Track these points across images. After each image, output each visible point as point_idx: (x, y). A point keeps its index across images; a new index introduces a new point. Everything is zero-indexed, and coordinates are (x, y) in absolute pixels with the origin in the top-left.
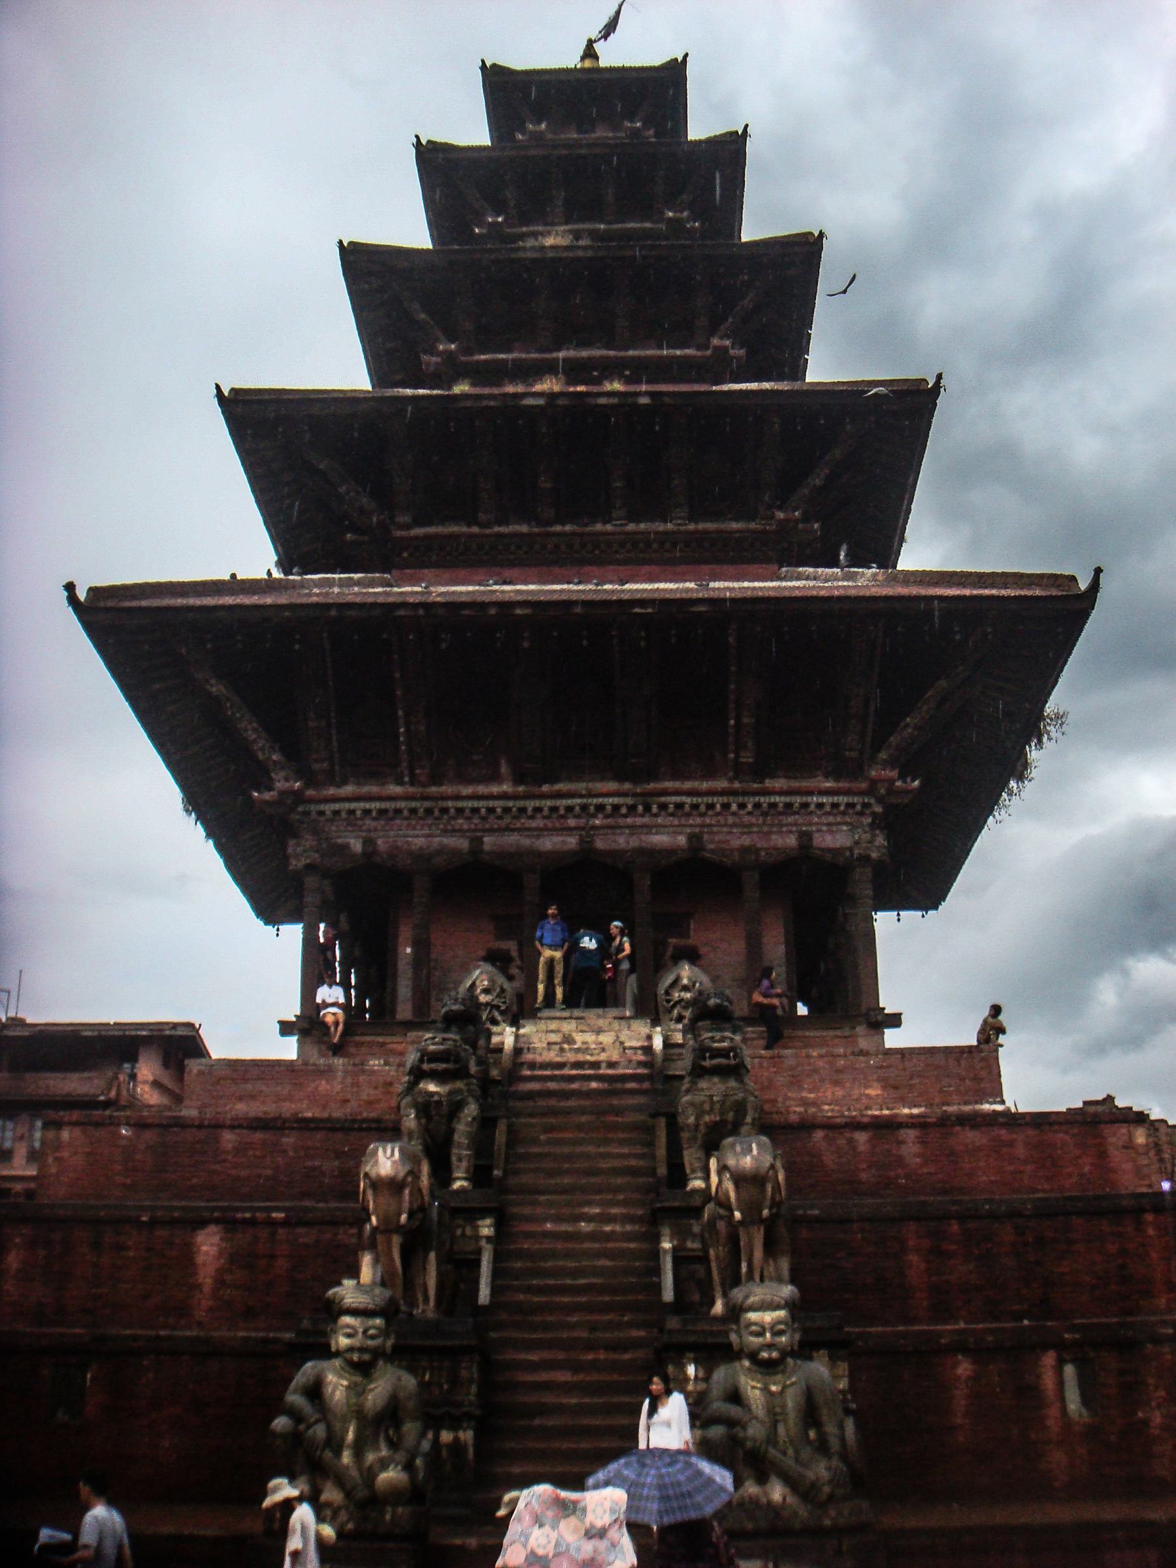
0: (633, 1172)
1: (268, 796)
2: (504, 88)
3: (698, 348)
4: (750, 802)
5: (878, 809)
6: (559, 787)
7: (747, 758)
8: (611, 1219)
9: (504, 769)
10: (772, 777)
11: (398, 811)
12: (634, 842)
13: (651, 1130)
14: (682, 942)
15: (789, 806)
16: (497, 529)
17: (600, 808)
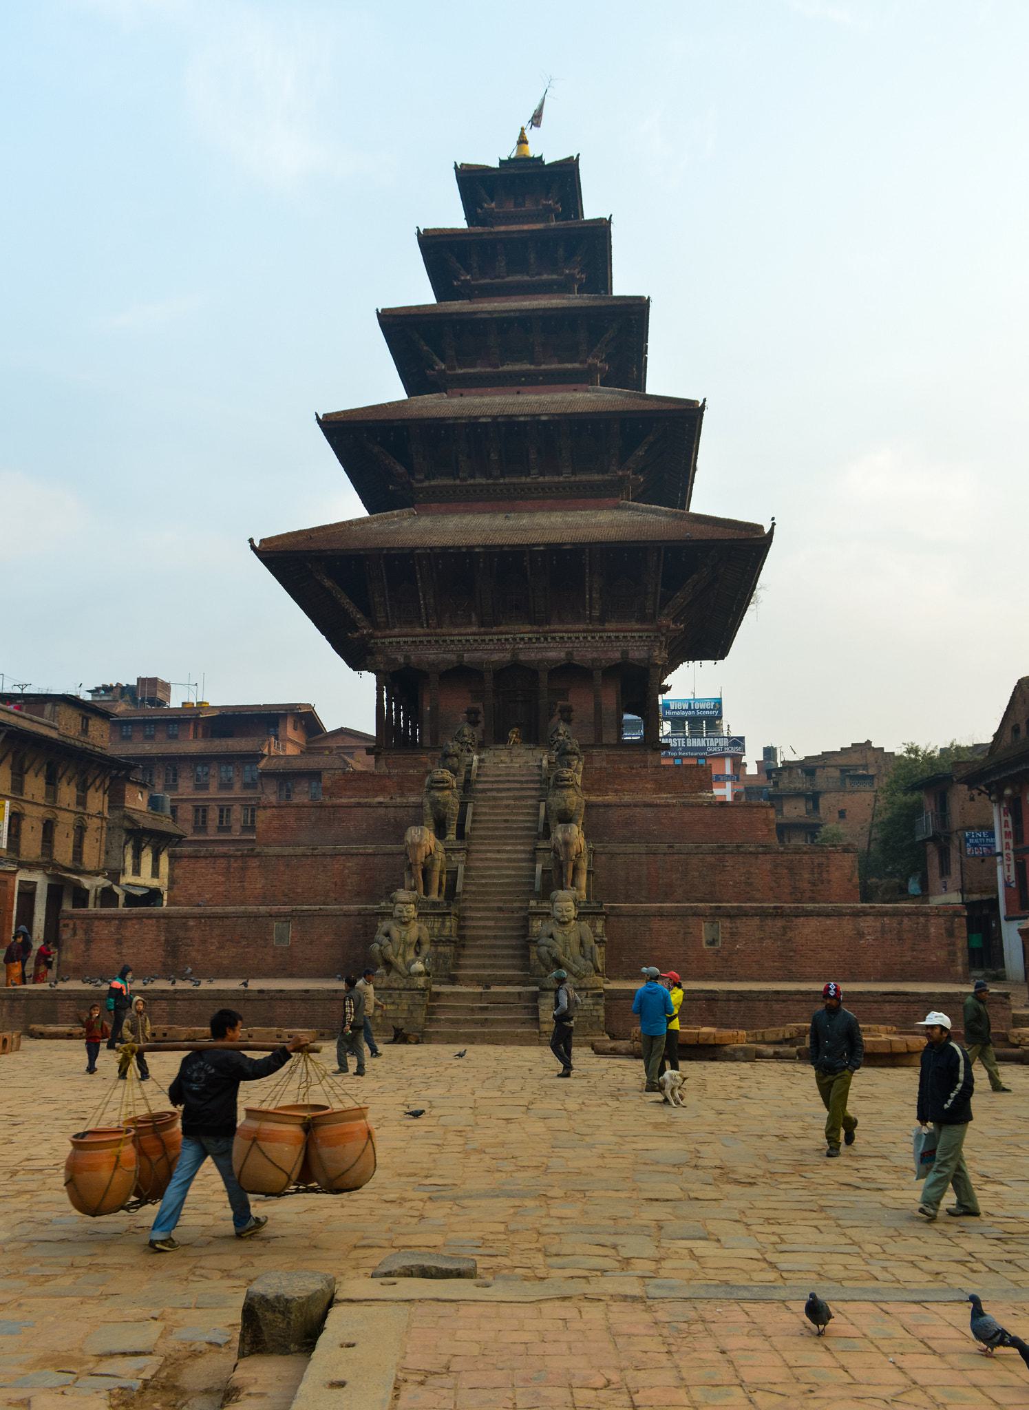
0: (528, 829)
1: (356, 635)
2: (473, 182)
3: (581, 363)
4: (597, 635)
5: (663, 639)
6: (501, 628)
7: (596, 613)
8: (516, 852)
9: (474, 619)
10: (609, 622)
11: (421, 642)
12: (539, 656)
13: (538, 809)
14: (566, 703)
15: (617, 637)
16: (471, 481)
17: (522, 639)
